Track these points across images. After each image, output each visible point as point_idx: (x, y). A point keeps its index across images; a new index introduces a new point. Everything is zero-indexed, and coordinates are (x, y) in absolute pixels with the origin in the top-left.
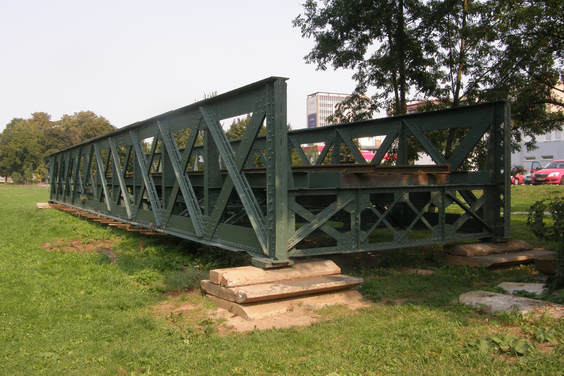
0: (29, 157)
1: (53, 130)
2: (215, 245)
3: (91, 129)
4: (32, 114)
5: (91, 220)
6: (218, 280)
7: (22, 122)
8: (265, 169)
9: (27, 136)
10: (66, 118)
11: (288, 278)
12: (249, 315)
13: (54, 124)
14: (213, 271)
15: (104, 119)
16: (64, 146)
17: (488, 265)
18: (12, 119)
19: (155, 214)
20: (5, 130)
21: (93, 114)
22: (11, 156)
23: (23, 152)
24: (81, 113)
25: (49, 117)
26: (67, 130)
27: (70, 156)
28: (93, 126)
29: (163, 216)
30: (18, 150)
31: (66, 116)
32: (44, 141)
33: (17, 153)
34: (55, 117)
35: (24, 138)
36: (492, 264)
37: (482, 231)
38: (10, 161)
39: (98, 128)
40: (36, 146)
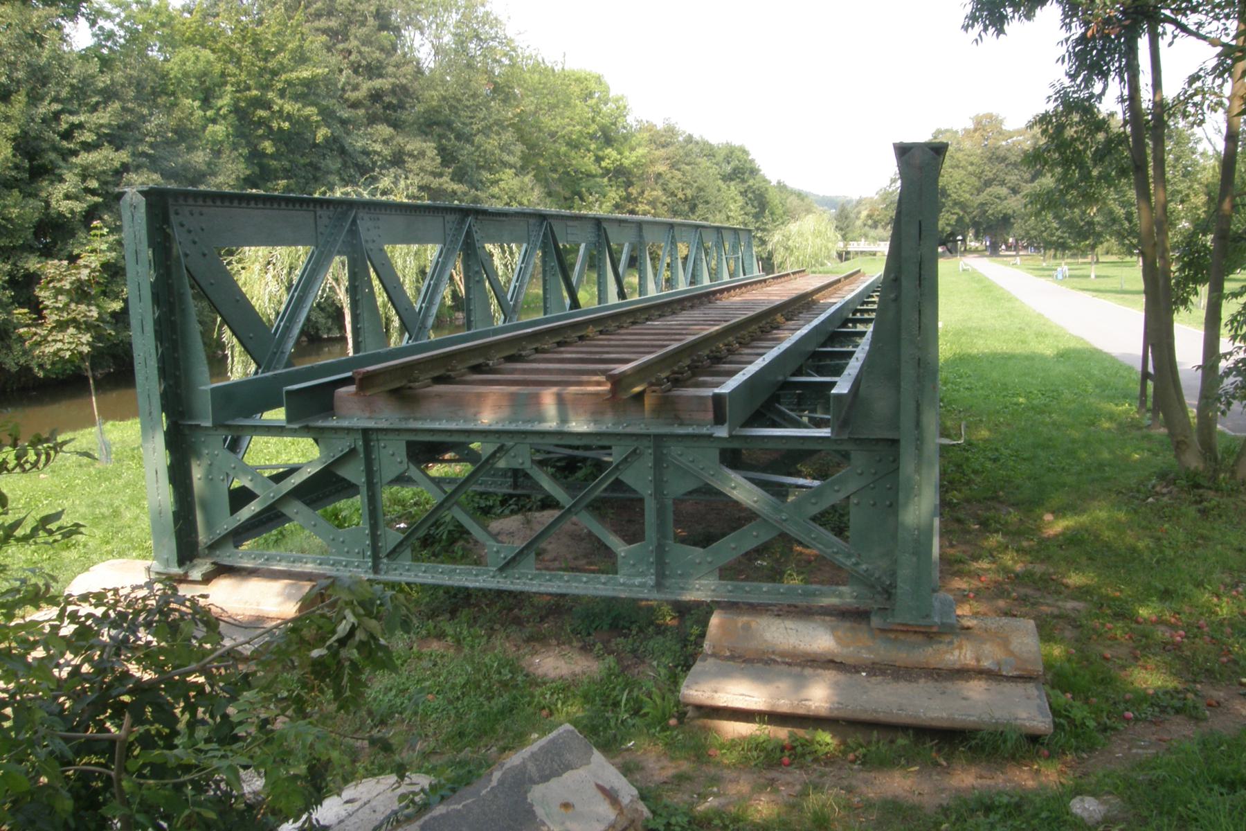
0: (950, 203)
18: (934, 131)
25: (1001, 122)
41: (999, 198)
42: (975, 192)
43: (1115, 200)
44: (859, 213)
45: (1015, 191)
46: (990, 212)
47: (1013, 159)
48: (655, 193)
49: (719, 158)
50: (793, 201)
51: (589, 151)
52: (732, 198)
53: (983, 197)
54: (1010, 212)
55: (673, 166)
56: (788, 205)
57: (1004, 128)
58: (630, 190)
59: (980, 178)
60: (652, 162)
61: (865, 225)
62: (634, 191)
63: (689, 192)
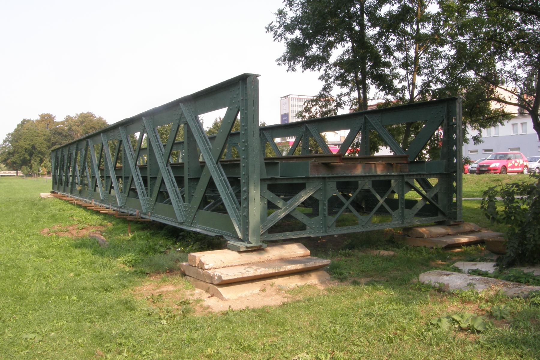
1: (57, 129)
2: (194, 230)
4: (39, 115)
5: (85, 208)
6: (196, 263)
7: (31, 122)
8: (239, 161)
9: (35, 134)
10: (68, 118)
11: (262, 260)
12: (224, 296)
13: (58, 123)
14: (191, 254)
15: (102, 118)
17: (444, 246)
18: (22, 120)
19: (142, 202)
20: (15, 129)
21: (92, 115)
22: (21, 152)
24: (82, 114)
25: (54, 118)
26: (70, 129)
27: (69, 151)
28: (92, 125)
29: (148, 204)
30: (27, 146)
31: (68, 116)
32: (50, 139)
33: (26, 149)
34: (60, 118)
36: (447, 245)
37: (437, 215)
38: (20, 157)
40: (42, 143)
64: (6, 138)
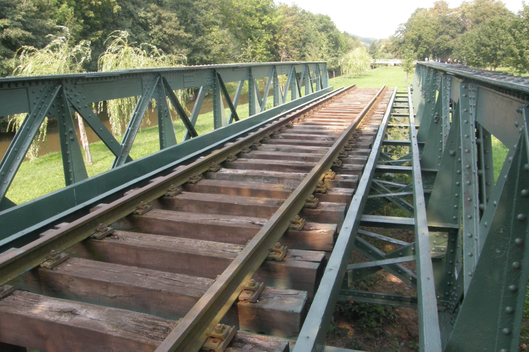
0: (423, 43)
3: (481, 15)
7: (423, 10)
16: (455, 32)
23: (418, 39)
26: (463, 16)
28: (483, 12)
30: (414, 37)
33: (413, 40)
35: (421, 26)
39: (489, 13)
40: (429, 33)
41: (446, 40)
42: (435, 38)
43: (514, 45)
44: (380, 46)
45: (453, 37)
46: (441, 47)
47: (453, 22)
48: (286, 37)
49: (317, 21)
50: (350, 41)
51: (256, 16)
52: (323, 39)
53: (437, 40)
54: (450, 47)
55: (295, 25)
56: (348, 43)
57: (448, 7)
58: (275, 35)
59: (437, 31)
60: (285, 23)
61: (383, 51)
62: (277, 36)
63: (302, 37)
64: (398, 29)
